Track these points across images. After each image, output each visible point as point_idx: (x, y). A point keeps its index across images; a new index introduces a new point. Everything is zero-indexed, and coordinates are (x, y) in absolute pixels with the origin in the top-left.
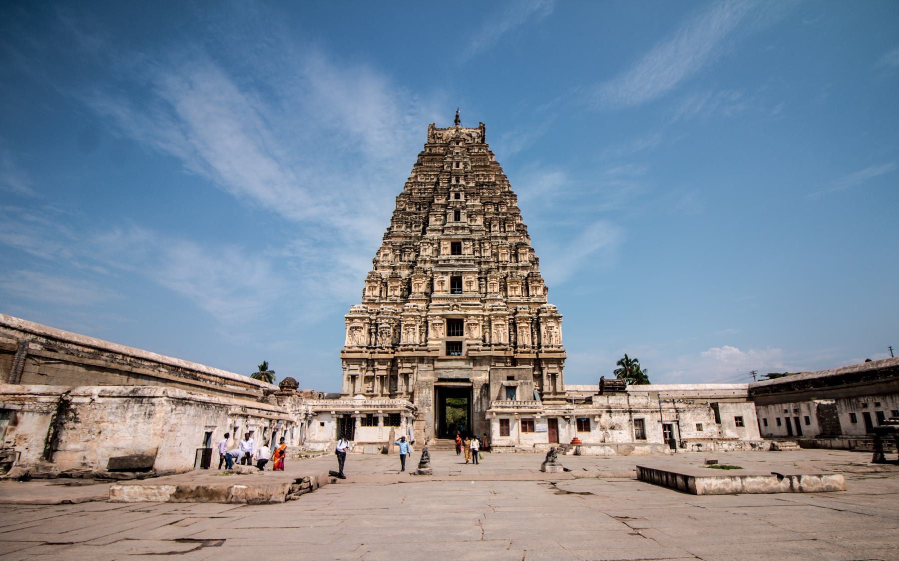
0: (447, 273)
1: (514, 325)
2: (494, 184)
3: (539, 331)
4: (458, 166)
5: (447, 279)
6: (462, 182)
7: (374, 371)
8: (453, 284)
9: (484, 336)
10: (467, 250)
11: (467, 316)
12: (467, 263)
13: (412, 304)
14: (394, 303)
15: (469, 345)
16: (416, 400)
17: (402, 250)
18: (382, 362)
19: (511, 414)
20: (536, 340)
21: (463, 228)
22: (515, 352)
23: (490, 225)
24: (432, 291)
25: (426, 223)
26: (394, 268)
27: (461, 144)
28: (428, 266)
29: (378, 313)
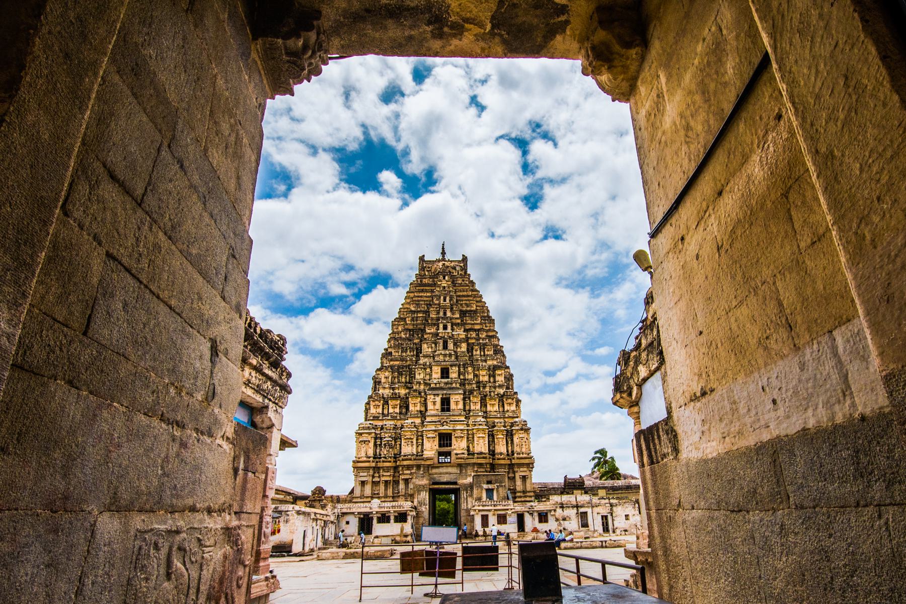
0: (438, 395)
1: (492, 436)
2: (475, 312)
3: (512, 440)
4: (445, 300)
5: (438, 399)
6: (449, 314)
7: (379, 477)
8: (443, 403)
9: (468, 447)
10: (454, 374)
11: (454, 430)
12: (454, 385)
13: (410, 421)
14: (394, 418)
15: (457, 454)
16: (416, 501)
17: (398, 371)
18: (387, 469)
19: (489, 510)
20: (510, 448)
21: (450, 355)
22: (494, 459)
23: (472, 349)
25: (419, 350)
26: (393, 389)
27: (447, 278)
28: (422, 387)
29: (382, 428)
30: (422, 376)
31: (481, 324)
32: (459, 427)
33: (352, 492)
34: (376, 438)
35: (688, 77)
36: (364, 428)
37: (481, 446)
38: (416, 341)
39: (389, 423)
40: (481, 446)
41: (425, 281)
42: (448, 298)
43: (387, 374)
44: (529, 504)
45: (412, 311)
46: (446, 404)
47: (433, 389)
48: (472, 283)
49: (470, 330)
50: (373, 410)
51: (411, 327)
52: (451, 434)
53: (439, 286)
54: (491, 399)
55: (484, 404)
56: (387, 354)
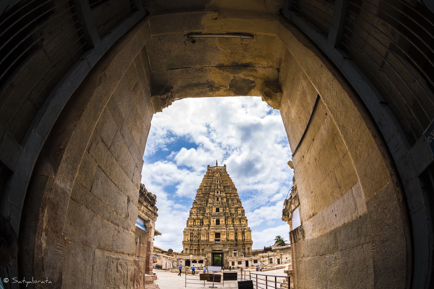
1: (236, 234)
2: (229, 186)
3: (244, 235)
5: (215, 220)
6: (219, 187)
13: (204, 228)
17: (199, 209)
21: (220, 203)
24: (210, 224)
25: (207, 201)
28: (209, 215)
29: (193, 230)
30: (208, 211)
31: (232, 191)
32: (223, 231)
33: (182, 252)
34: (191, 234)
35: (297, 102)
36: (186, 230)
37: (232, 237)
38: (206, 198)
39: (196, 229)
40: (232, 237)
41: (210, 175)
42: (219, 181)
43: (195, 210)
44: (250, 257)
45: (204, 186)
46: (218, 222)
47: (213, 216)
48: (228, 175)
49: (228, 193)
50: (190, 224)
51: (204, 192)
52: (220, 233)
53: (215, 176)
54: (236, 219)
55: (233, 221)
56: (195, 203)
